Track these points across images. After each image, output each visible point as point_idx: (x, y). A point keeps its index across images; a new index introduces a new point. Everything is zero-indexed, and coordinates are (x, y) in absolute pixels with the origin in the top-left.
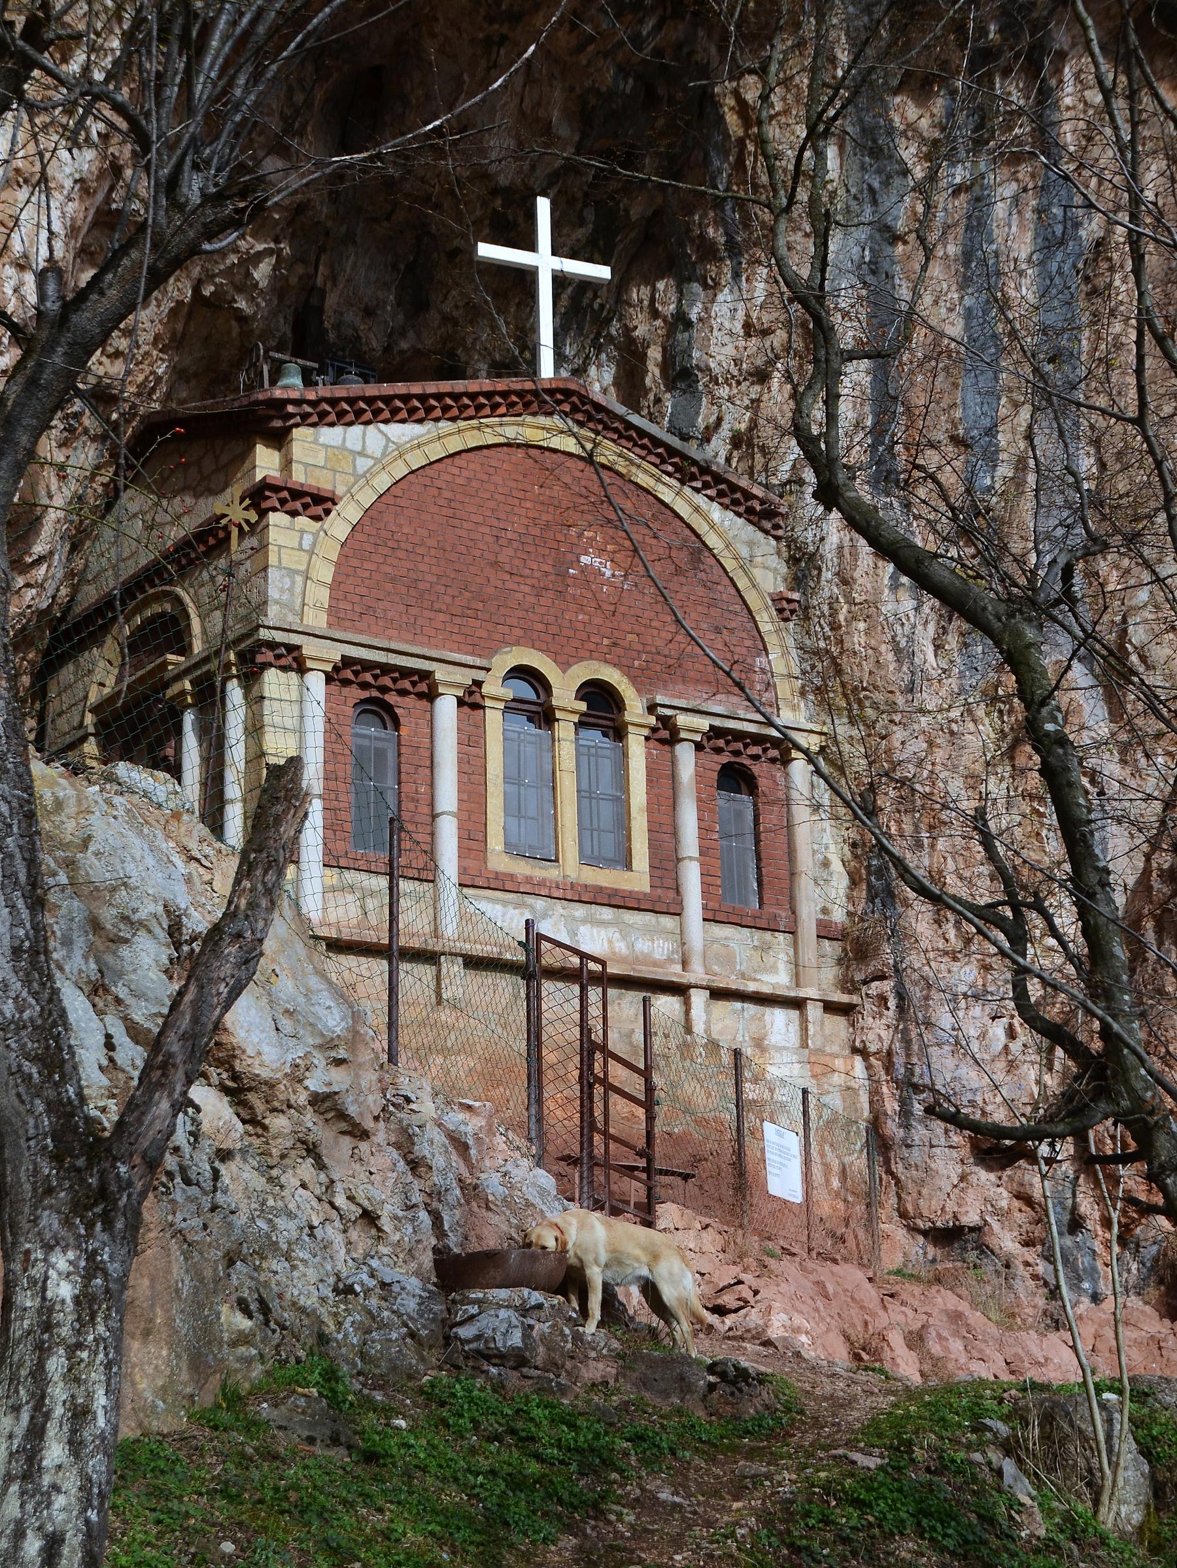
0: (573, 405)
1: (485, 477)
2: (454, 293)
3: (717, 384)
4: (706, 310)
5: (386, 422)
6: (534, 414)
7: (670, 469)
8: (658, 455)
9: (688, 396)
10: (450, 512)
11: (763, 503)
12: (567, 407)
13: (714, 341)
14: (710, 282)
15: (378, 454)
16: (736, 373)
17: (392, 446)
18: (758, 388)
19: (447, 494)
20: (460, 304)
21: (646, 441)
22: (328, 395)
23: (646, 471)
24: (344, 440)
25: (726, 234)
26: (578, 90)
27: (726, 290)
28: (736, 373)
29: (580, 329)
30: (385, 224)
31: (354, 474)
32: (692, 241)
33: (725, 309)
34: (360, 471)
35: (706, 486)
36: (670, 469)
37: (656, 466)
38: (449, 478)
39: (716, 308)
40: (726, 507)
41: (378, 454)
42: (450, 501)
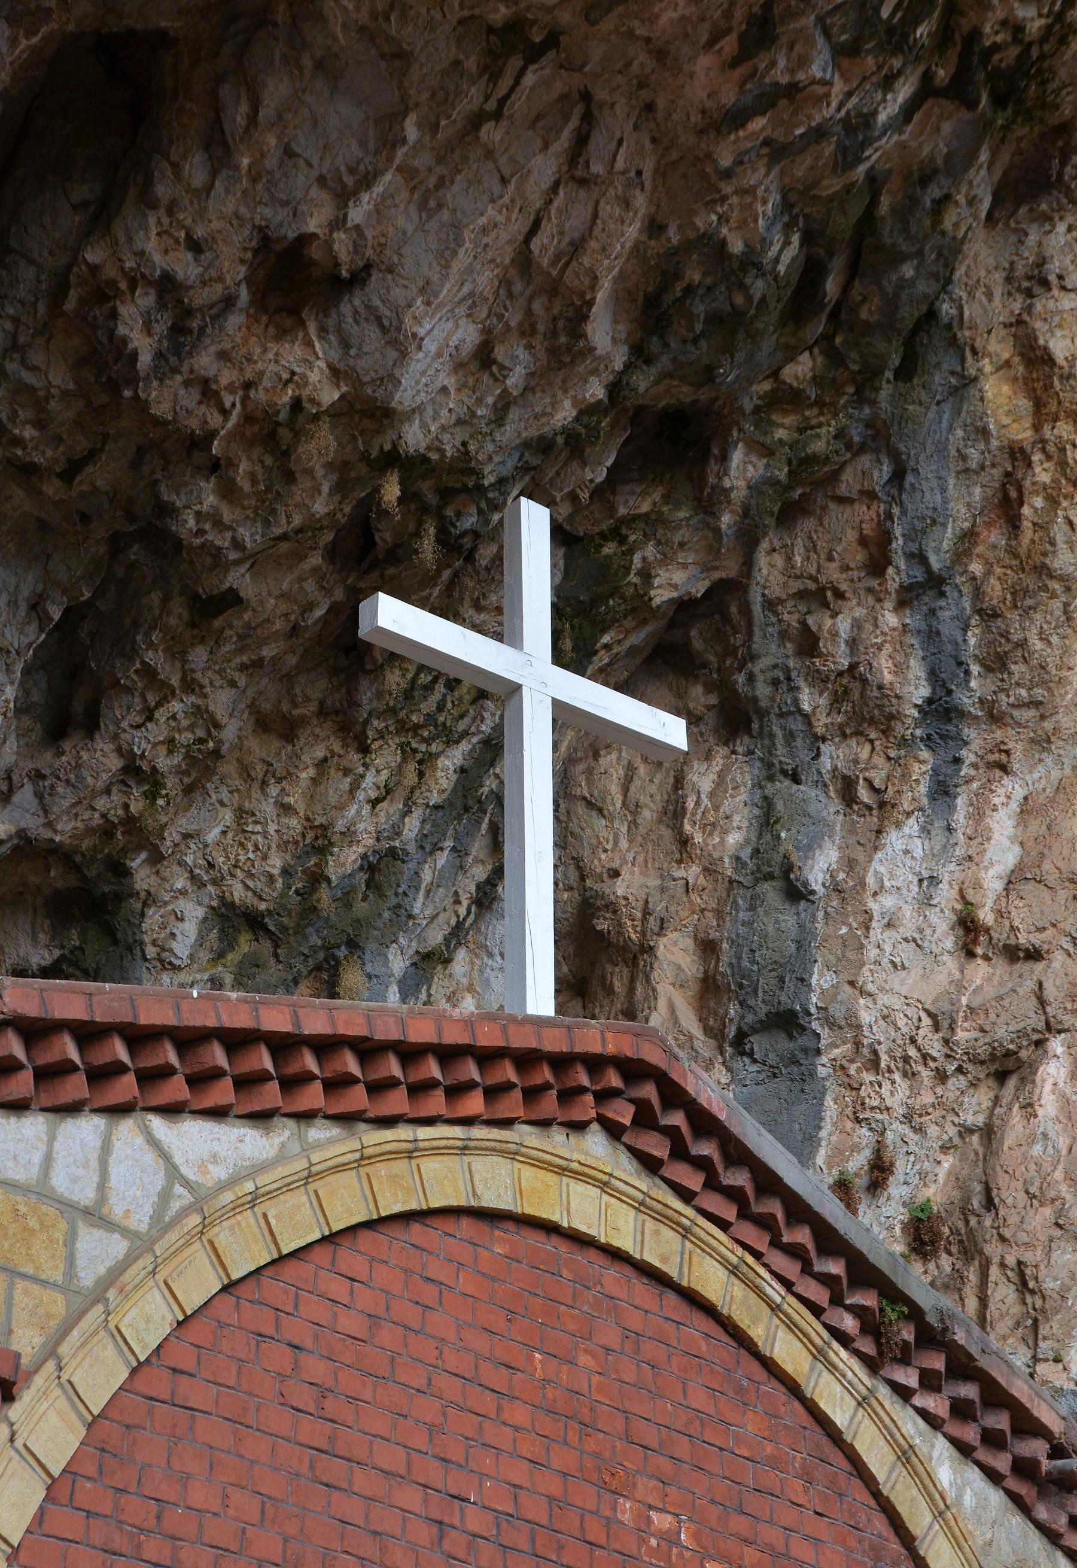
0: (643, 1108)
1: (412, 1315)
2: (176, 706)
3: (874, 1064)
4: (850, 864)
5: (172, 1110)
6: (544, 1124)
7: (849, 1323)
8: (827, 1280)
9: (781, 1085)
10: (312, 1430)
11: (1058, 1451)
12: (623, 1113)
13: (872, 953)
14: (864, 794)
15: (140, 1221)
16: (935, 1048)
17: (182, 1197)
18: (983, 1096)
19: (316, 1368)
20: (186, 737)
21: (802, 1236)
22: (31, 1009)
23: (792, 1326)
24: (48, 1160)
25: (933, 676)
26: (673, 235)
27: (912, 826)
28: (935, 1048)
29: (459, 852)
30: (51, 488)
31: (67, 1287)
32: (819, 680)
33: (905, 877)
34: (88, 1276)
35: (930, 1382)
36: (849, 1323)
37: (816, 1310)
38: (314, 1308)
39: (878, 867)
40: (964, 1449)
41: (140, 1221)
42: (324, 1392)
